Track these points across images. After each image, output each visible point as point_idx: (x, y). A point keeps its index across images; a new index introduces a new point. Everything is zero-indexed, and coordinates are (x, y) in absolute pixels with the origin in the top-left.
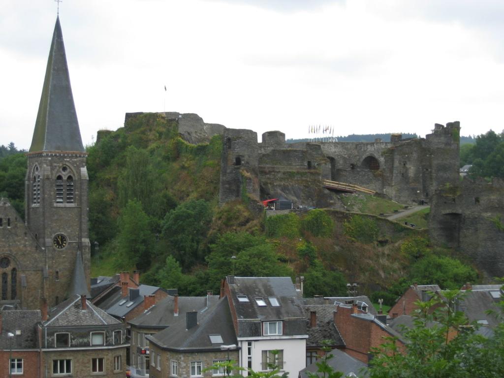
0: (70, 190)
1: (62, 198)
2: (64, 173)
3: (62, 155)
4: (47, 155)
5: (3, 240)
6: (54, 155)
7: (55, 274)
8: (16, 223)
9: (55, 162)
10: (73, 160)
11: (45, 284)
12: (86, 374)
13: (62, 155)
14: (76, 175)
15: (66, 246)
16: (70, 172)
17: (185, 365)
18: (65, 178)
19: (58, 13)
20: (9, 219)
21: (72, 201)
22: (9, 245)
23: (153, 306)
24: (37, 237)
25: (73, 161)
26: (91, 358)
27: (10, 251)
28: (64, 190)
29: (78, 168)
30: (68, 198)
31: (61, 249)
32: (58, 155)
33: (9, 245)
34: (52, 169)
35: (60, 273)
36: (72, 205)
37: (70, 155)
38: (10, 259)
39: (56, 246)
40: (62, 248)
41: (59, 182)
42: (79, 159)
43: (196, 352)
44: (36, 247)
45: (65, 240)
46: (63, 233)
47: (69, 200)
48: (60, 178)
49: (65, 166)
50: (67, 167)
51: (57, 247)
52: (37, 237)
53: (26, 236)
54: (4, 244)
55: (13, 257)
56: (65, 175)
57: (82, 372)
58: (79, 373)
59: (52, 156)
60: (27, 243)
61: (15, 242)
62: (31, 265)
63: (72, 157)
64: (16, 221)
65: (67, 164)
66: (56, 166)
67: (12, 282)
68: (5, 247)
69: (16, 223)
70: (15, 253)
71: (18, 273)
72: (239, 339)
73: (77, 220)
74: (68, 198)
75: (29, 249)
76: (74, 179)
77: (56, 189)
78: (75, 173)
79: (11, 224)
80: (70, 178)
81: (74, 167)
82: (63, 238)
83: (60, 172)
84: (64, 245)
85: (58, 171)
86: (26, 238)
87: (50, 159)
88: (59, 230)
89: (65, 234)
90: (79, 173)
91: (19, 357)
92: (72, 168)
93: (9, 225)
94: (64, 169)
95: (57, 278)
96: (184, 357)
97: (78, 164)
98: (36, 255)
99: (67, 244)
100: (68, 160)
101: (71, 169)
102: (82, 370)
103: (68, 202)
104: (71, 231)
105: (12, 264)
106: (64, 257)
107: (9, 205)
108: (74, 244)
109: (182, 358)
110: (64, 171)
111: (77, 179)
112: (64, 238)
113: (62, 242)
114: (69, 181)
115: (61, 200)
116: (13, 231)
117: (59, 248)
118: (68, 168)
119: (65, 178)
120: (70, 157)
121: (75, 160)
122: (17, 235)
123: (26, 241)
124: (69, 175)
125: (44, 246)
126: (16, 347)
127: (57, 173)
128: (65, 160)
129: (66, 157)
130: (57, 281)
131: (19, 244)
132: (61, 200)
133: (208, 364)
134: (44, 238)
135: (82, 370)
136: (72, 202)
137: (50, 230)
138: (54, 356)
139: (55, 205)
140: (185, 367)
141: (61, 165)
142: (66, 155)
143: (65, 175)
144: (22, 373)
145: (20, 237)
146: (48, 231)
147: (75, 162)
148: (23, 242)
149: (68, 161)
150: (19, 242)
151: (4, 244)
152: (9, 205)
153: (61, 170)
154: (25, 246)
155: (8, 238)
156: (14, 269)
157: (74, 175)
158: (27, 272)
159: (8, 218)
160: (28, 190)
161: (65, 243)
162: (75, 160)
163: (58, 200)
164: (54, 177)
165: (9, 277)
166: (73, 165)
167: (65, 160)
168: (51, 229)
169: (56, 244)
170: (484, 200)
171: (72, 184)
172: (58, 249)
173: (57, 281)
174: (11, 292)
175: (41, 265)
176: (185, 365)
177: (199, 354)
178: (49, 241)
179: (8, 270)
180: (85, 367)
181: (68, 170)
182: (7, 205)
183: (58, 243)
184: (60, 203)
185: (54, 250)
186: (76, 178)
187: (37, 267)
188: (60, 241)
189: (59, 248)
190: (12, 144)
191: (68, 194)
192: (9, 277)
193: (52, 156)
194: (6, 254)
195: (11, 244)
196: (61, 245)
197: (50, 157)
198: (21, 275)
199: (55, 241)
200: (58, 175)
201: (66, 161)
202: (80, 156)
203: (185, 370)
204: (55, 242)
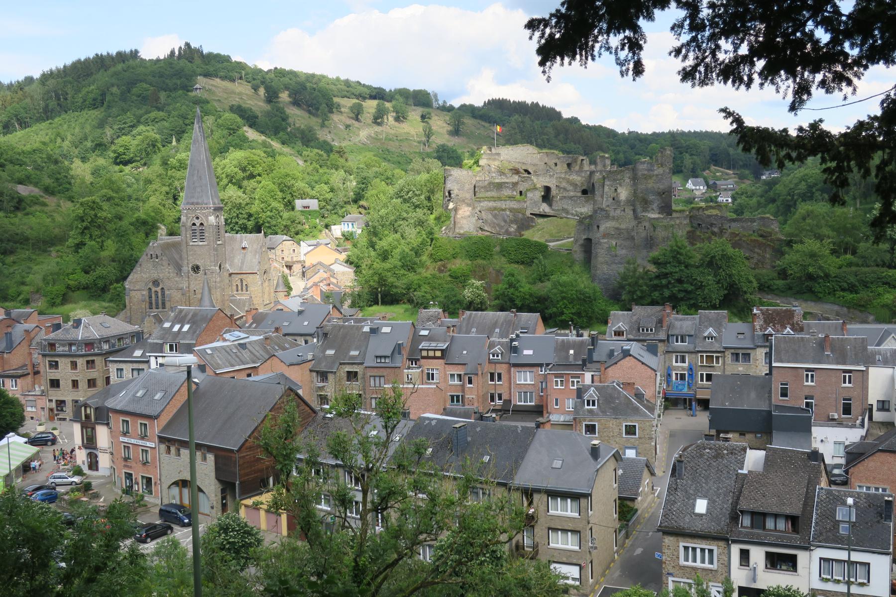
0: (202, 232)
18: (198, 225)
24: (179, 268)
29: (207, 217)
47: (202, 240)
48: (194, 224)
52: (179, 268)
56: (198, 222)
72: (147, 354)
75: (172, 274)
80: (202, 224)
94: (198, 218)
98: (177, 279)
116: (160, 262)
119: (198, 225)
143: (198, 222)
147: (205, 213)
154: (169, 273)
156: (163, 288)
164: (189, 224)
170: (602, 228)
179: (159, 289)
183: (195, 271)
188: (196, 269)
198: (167, 292)
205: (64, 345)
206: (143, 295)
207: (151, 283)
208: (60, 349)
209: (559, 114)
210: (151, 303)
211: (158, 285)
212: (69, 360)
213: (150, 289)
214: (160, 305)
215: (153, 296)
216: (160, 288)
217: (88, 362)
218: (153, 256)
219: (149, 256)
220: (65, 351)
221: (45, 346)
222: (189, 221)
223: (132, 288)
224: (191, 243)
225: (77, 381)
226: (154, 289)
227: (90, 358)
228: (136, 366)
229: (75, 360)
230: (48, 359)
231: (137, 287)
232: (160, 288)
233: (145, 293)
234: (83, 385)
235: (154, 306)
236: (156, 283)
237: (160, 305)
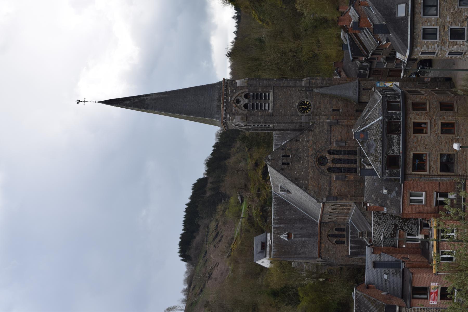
0: (257, 96)
1: (265, 104)
2: (241, 103)
3: (225, 104)
4: (225, 118)
5: (302, 162)
6: (224, 112)
7: (335, 112)
8: (287, 149)
9: (232, 110)
10: (229, 93)
11: (343, 124)
12: (428, 140)
13: (225, 104)
14: (243, 90)
15: (309, 101)
16: (241, 96)
17: (425, 46)
19: (96, 102)
20: (283, 156)
21: (267, 94)
22: (307, 156)
23: (368, 19)
25: (231, 93)
26: (412, 135)
27: (312, 155)
28: (258, 102)
29: (237, 88)
30: (265, 98)
31: (312, 105)
32: (224, 108)
33: (307, 156)
34: (238, 114)
35: (335, 108)
36: (271, 94)
37: (225, 96)
38: (319, 156)
39: (309, 111)
40: (310, 106)
41: (250, 107)
42: (228, 87)
43: (413, 34)
44: (309, 130)
45: (304, 102)
46: (297, 104)
47: (266, 98)
48: (246, 106)
49: (235, 101)
50: (236, 99)
51: (309, 109)
53: (299, 140)
54: (305, 161)
55: (318, 153)
56: (244, 101)
57: (426, 143)
58: (427, 147)
59: (226, 114)
60: (305, 140)
61: (304, 151)
62: (326, 136)
63: (227, 95)
64: (285, 149)
65: (233, 99)
66: (235, 110)
67: (341, 154)
68: (309, 161)
69: (287, 149)
70: (314, 151)
71: (332, 149)
73: (285, 90)
74: (265, 98)
75: (310, 138)
76: (247, 93)
77: (256, 110)
78: (241, 91)
79: (288, 155)
80: (246, 96)
81: (236, 92)
82: (302, 104)
83: (240, 106)
84: (308, 103)
85: (240, 108)
86: (301, 141)
87: (228, 116)
88: (294, 108)
89: (298, 101)
90: (242, 87)
91: (408, 195)
92: (236, 94)
93: (289, 156)
94: (238, 101)
95: (338, 110)
96: (417, 47)
97: (233, 89)
98: (317, 131)
99: (308, 100)
100: (229, 98)
101: (238, 95)
102: (424, 144)
103: (269, 99)
104: (296, 96)
105: (324, 154)
106: (320, 103)
107: (270, 156)
108: (307, 93)
109: (418, 48)
110: (240, 101)
111: (247, 90)
112: (301, 103)
113: (306, 105)
114: (249, 97)
115: (267, 105)
116: (294, 152)
117: (310, 108)
118: (237, 98)
119: (246, 101)
120: (227, 96)
121: (230, 91)
122: (298, 149)
123: (303, 140)
124: (243, 97)
125: (309, 123)
126: (399, 198)
127: (241, 109)
128: (229, 101)
129: (227, 100)
130: (341, 110)
131: (306, 147)
132: (267, 105)
133: (426, 21)
134: (301, 123)
135: (424, 144)
136: (269, 95)
137: (294, 117)
138: (409, 171)
139: (271, 111)
140: (428, 47)
141: (234, 105)
142: (225, 100)
143: (244, 101)
144: (424, 193)
145: (300, 146)
146: (295, 119)
147: (232, 91)
148: (304, 143)
149: (231, 98)
150: (304, 147)
151: (305, 161)
152: (270, 156)
153: (238, 105)
154: (308, 141)
155: (300, 158)
156: (329, 152)
157: (243, 92)
158: (332, 140)
159: (282, 157)
160: (258, 130)
161: (307, 102)
162: (230, 91)
163: (267, 108)
164: (245, 112)
165: (336, 157)
166: (234, 93)
167: (229, 101)
168: (293, 115)
169: (307, 111)
171: (252, 94)
172: (312, 109)
173: (341, 110)
174: (350, 156)
175: (326, 126)
176: (425, 46)
177: (415, 31)
178: (304, 119)
180: (421, 140)
181: (239, 98)
182: (270, 158)
184: (270, 106)
185: (312, 113)
186: (246, 91)
187: (327, 131)
188: (303, 107)
189: (310, 108)
190: (224, 78)
191: (261, 98)
192: (336, 157)
193: (226, 114)
194: (315, 160)
195: (305, 155)
196: (308, 108)
197: (226, 116)
198: (334, 146)
199: (304, 112)
200: (243, 108)
201: (231, 100)
202: (226, 86)
203: (430, 46)
204: (305, 111)
205: (391, 143)
206: (337, 178)
207: (322, 167)
208: (397, 149)
209: (200, 181)
210: (349, 170)
211: (324, 158)
212: (412, 137)
213: (329, 169)
214: (352, 157)
215: (338, 165)
216: (328, 156)
217: (416, 131)
218: (285, 161)
219: (285, 166)
220: (399, 140)
221: (391, 175)
222: (241, 111)
223: (327, 193)
224: (271, 111)
225: (443, 124)
226: (330, 164)
227: (410, 106)
228: (420, 9)
229: (411, 125)
230: (410, 170)
231: (326, 186)
232: (328, 156)
233: (334, 176)
234: (449, 118)
235: (353, 166)
236: (321, 161)
237: (352, 157)
